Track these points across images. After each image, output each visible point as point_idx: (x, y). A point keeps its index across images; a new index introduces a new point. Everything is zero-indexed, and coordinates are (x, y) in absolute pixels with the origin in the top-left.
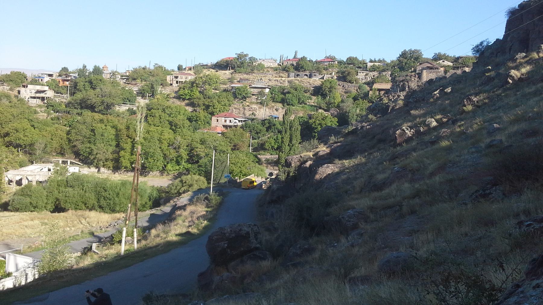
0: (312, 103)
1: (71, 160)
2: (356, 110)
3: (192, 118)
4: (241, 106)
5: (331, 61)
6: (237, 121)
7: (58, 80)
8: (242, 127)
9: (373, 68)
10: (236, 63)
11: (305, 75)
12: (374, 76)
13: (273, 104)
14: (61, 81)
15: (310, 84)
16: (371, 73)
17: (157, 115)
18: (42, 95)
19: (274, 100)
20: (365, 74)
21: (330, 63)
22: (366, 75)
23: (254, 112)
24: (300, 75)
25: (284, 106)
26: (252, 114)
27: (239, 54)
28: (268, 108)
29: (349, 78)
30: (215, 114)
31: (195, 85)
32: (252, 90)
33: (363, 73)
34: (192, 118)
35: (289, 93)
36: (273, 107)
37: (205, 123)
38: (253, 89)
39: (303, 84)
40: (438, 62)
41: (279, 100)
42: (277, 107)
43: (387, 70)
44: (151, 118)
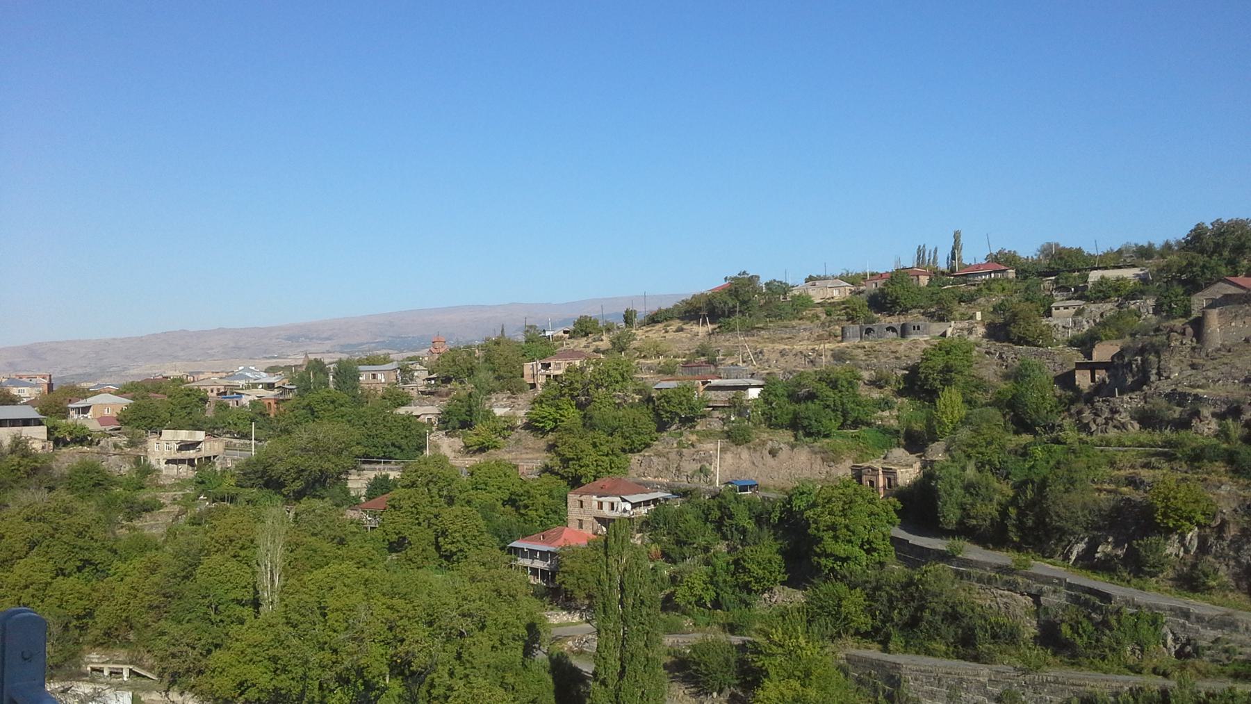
0: (892, 421)
1: (131, 667)
2: (964, 469)
3: (517, 498)
4: (675, 445)
5: (995, 272)
6: (628, 507)
7: (266, 402)
8: (646, 524)
9: (1100, 291)
10: (726, 303)
11: (888, 329)
12: (1102, 315)
13: (765, 436)
14: (272, 402)
15: (897, 358)
16: (1093, 307)
17: (406, 504)
18: (191, 454)
19: (772, 422)
20: (1072, 311)
21: (993, 275)
22: (1079, 312)
23: (705, 463)
24: (876, 329)
25: (796, 436)
26: (701, 470)
27: (735, 278)
28: (749, 448)
29: (1014, 330)
30: (583, 480)
32: (712, 395)
33: (1066, 308)
34: (517, 498)
35: (811, 397)
36: (764, 443)
37: (547, 514)
38: (713, 392)
39: (876, 358)
41: (786, 419)
42: (776, 446)
43: (1142, 292)
44: (392, 515)
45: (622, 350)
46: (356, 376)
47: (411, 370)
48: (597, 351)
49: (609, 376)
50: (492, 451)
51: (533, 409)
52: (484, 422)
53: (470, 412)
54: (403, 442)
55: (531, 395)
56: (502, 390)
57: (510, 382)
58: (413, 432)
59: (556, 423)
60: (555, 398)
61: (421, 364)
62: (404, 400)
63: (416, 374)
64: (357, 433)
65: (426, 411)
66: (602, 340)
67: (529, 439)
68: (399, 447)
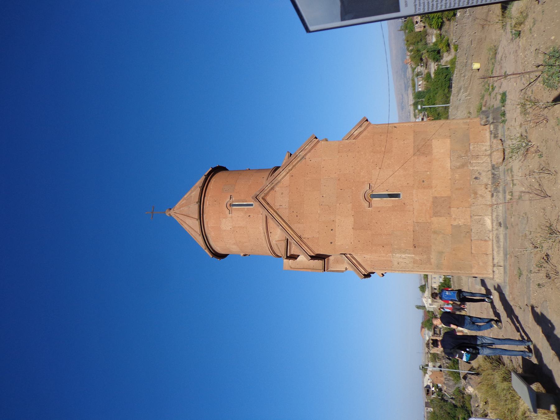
46: (420, 92)
47: (418, 72)
50: (449, 41)
51: (433, 27)
52: (438, 45)
53: (434, 51)
54: (445, 75)
55: (428, 27)
56: (426, 39)
57: (423, 35)
58: (441, 71)
59: (440, 18)
61: (415, 68)
62: (429, 74)
63: (419, 71)
64: (440, 92)
65: (433, 67)
67: (445, 28)
68: (447, 75)
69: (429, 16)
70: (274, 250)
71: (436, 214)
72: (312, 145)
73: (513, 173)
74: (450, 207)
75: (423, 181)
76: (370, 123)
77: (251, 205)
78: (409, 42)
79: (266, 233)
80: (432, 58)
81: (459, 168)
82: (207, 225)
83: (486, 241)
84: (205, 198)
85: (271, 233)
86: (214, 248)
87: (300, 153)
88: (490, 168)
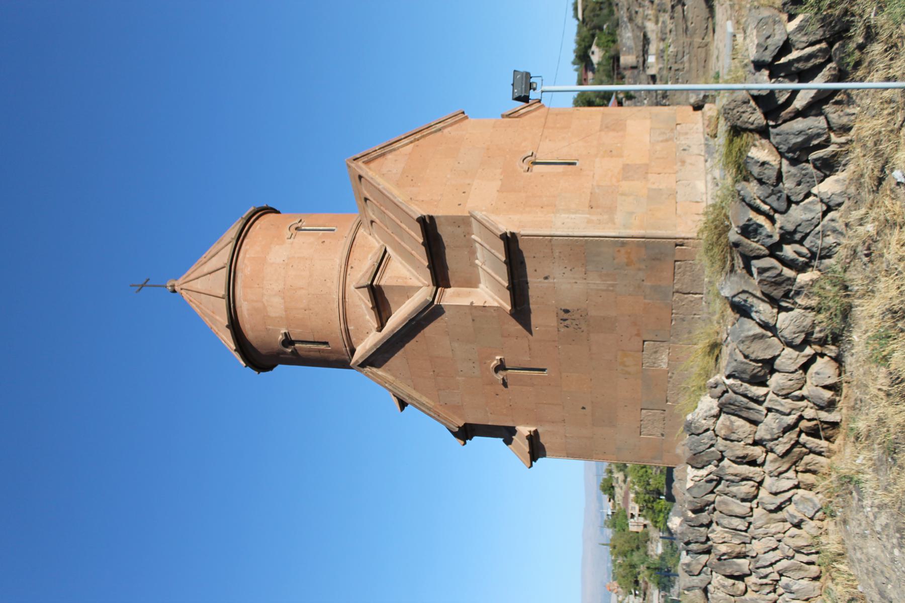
31: (649, 505)
40: (596, 66)
45: (625, 466)
48: (625, 481)
49: (642, 476)
53: (658, 569)
55: (651, 528)
56: (646, 547)
57: (640, 542)
60: (654, 512)
61: (624, 599)
66: (618, 478)
69: (653, 507)
70: (347, 308)
71: (626, 178)
72: (457, 119)
73: (754, 322)
74: (647, 173)
75: (611, 151)
76: (543, 106)
77: (333, 230)
78: (616, 550)
79: (343, 266)
80: (656, 581)
81: (662, 141)
82: (245, 254)
83: (697, 202)
84: (257, 222)
85: (352, 268)
86: (238, 304)
87: (437, 124)
88: (703, 141)
